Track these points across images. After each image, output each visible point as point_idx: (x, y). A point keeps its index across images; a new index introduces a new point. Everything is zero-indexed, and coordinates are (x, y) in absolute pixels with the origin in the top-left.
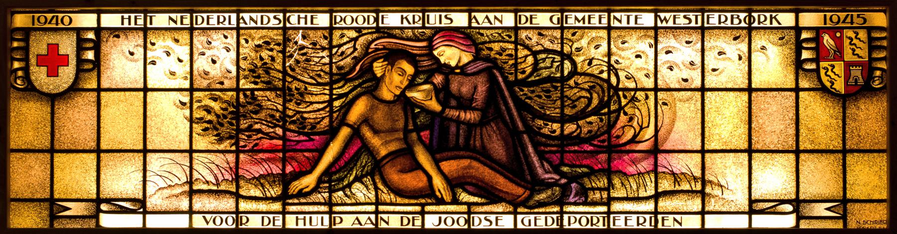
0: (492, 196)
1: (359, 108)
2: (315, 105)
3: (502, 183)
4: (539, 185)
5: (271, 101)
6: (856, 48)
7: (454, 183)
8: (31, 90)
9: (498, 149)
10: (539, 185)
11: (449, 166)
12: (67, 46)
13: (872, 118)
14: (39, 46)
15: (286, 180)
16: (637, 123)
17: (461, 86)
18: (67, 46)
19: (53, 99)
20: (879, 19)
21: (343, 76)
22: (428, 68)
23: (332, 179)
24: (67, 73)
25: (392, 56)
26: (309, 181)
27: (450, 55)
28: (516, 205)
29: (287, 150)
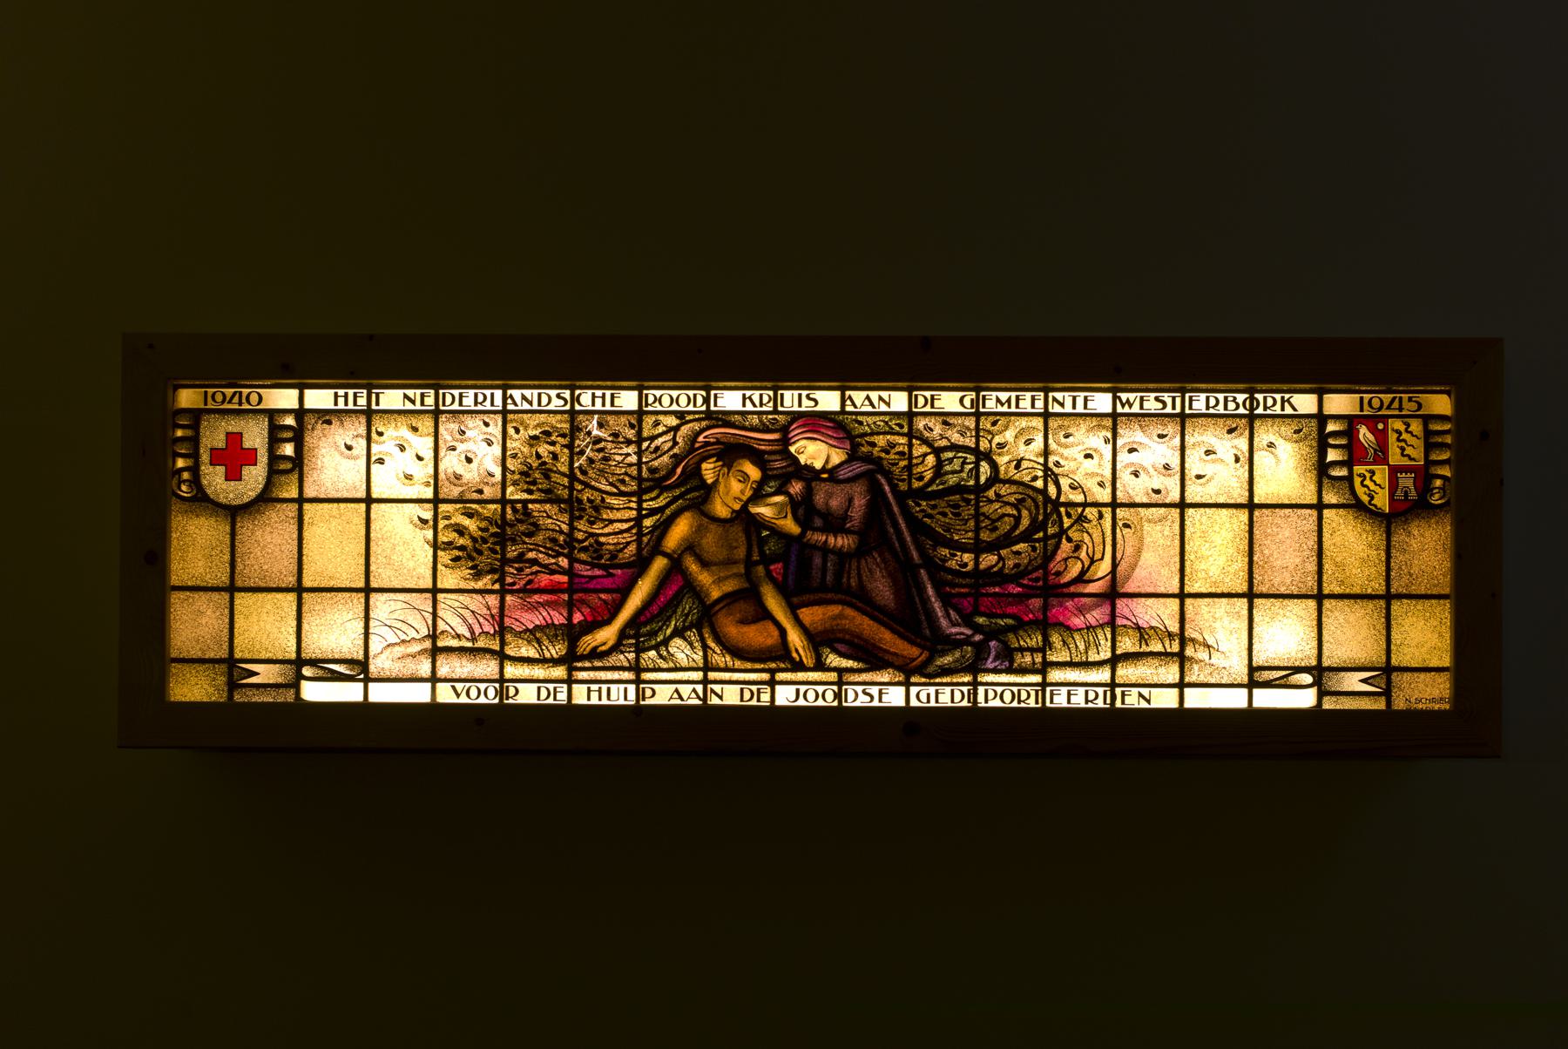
0: (873, 658)
1: (680, 530)
2: (617, 524)
3: (887, 639)
4: (938, 643)
5: (553, 519)
6: (1406, 445)
7: (819, 640)
8: (202, 500)
9: (882, 589)
10: (938, 643)
11: (809, 615)
12: (255, 436)
13: (1428, 549)
14: (214, 436)
15: (572, 634)
16: (1088, 553)
17: (830, 498)
18: (255, 436)
19: (234, 513)
20: (1441, 404)
21: (652, 482)
22: (782, 471)
23: (641, 633)
24: (255, 476)
25: (730, 453)
26: (606, 635)
27: (813, 452)
28: (909, 672)
29: (575, 590)
